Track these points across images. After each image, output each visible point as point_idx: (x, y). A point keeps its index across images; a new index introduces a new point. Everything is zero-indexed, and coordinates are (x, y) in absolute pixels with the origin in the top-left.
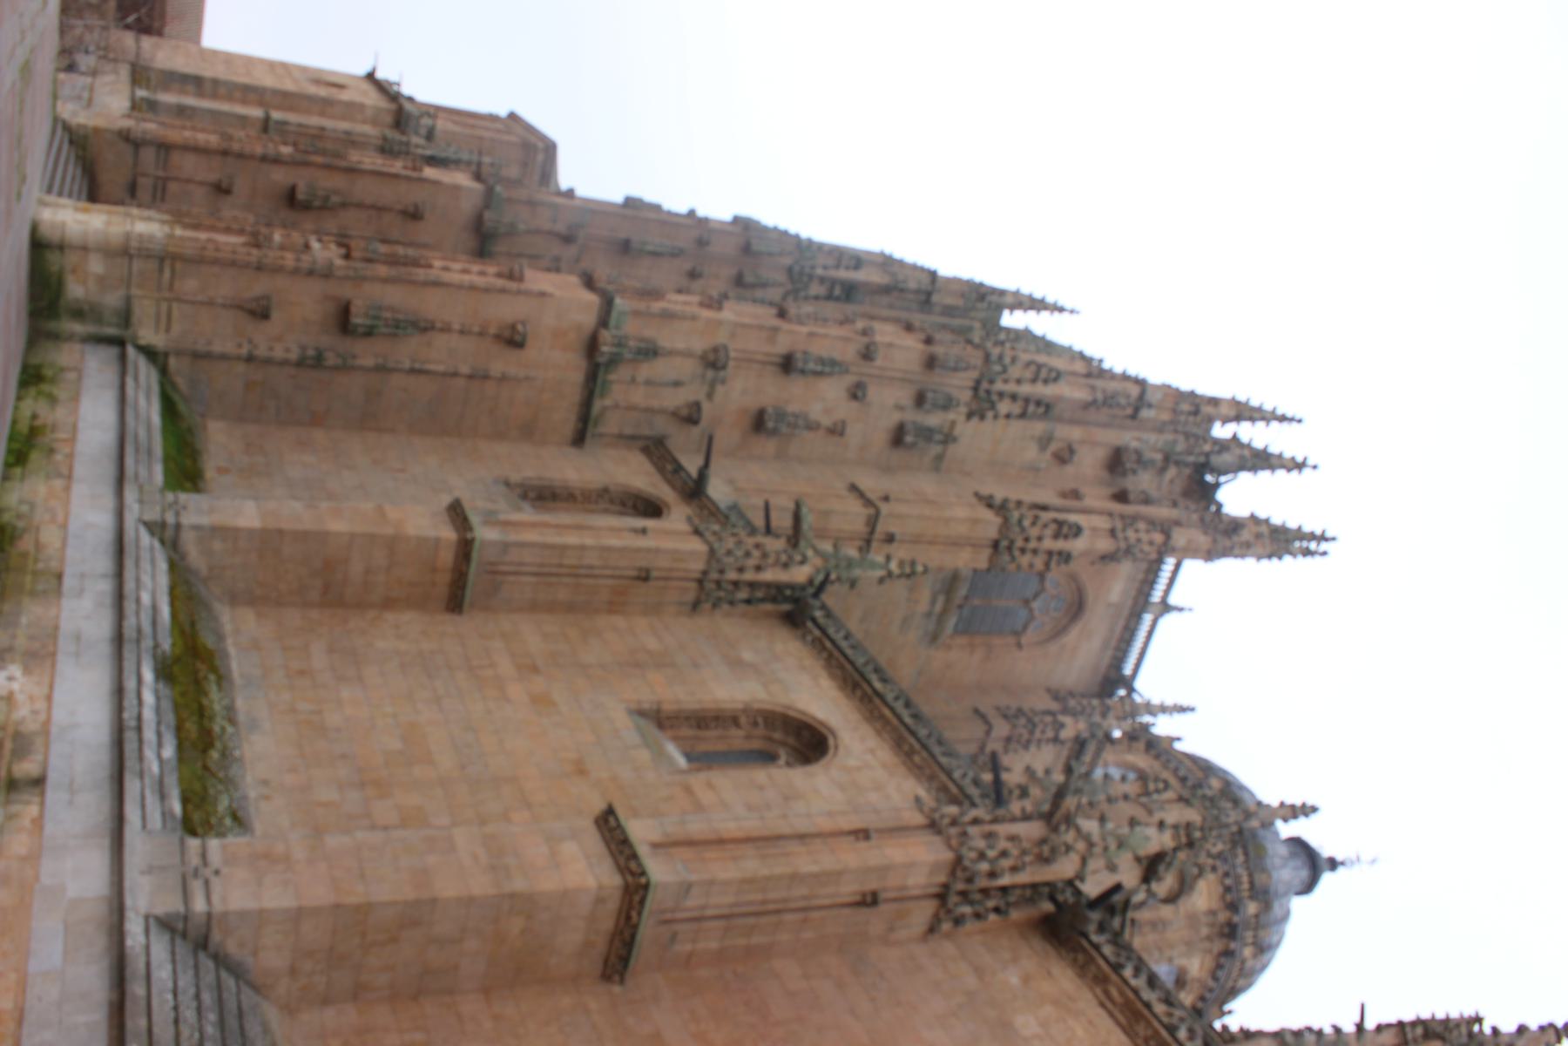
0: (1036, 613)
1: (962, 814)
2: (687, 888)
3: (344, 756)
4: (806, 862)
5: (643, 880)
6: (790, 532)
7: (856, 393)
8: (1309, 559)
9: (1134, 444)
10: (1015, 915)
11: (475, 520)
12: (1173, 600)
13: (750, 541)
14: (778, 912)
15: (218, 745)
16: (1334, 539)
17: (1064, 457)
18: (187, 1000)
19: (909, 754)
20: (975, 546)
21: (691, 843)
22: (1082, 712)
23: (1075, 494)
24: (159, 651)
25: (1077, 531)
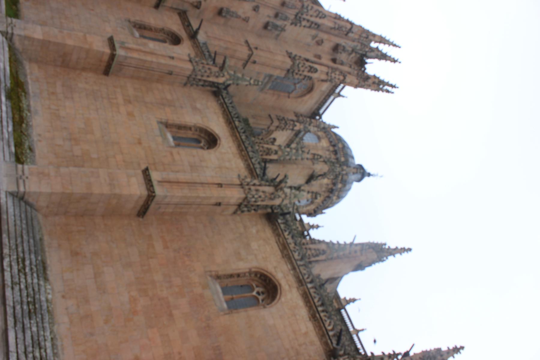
0: (297, 88)
1: (251, 181)
2: (166, 197)
3: (65, 128)
4: (202, 193)
5: (154, 194)
6: (221, 65)
7: (256, 9)
8: (387, 94)
9: (344, 44)
10: (260, 211)
11: (117, 45)
12: (342, 93)
13: (207, 67)
14: (191, 204)
15: (25, 122)
16: (398, 88)
17: (320, 43)
18: (18, 218)
19: (241, 151)
20: (282, 69)
21: (169, 182)
22: (303, 122)
23: (319, 57)
24: (7, 87)
25: (316, 71)
